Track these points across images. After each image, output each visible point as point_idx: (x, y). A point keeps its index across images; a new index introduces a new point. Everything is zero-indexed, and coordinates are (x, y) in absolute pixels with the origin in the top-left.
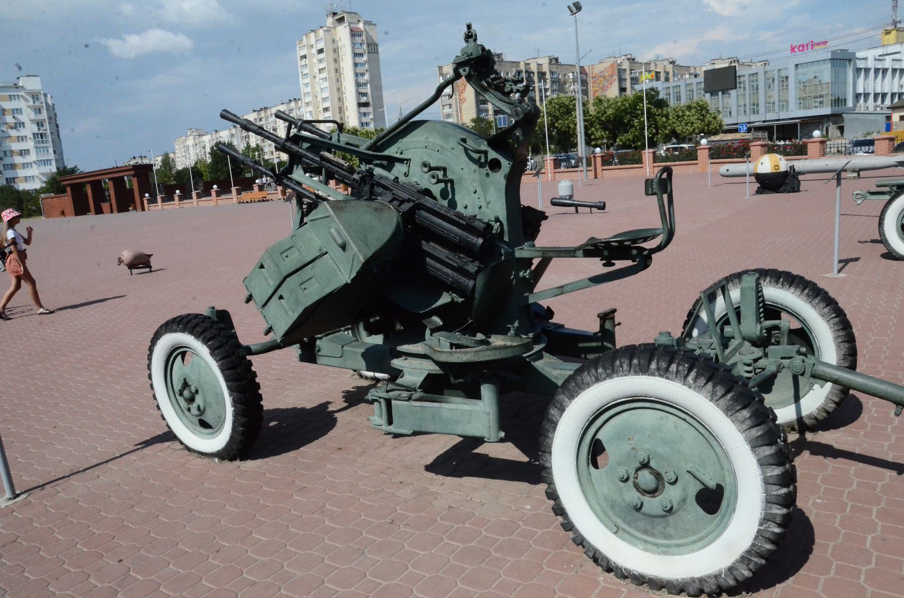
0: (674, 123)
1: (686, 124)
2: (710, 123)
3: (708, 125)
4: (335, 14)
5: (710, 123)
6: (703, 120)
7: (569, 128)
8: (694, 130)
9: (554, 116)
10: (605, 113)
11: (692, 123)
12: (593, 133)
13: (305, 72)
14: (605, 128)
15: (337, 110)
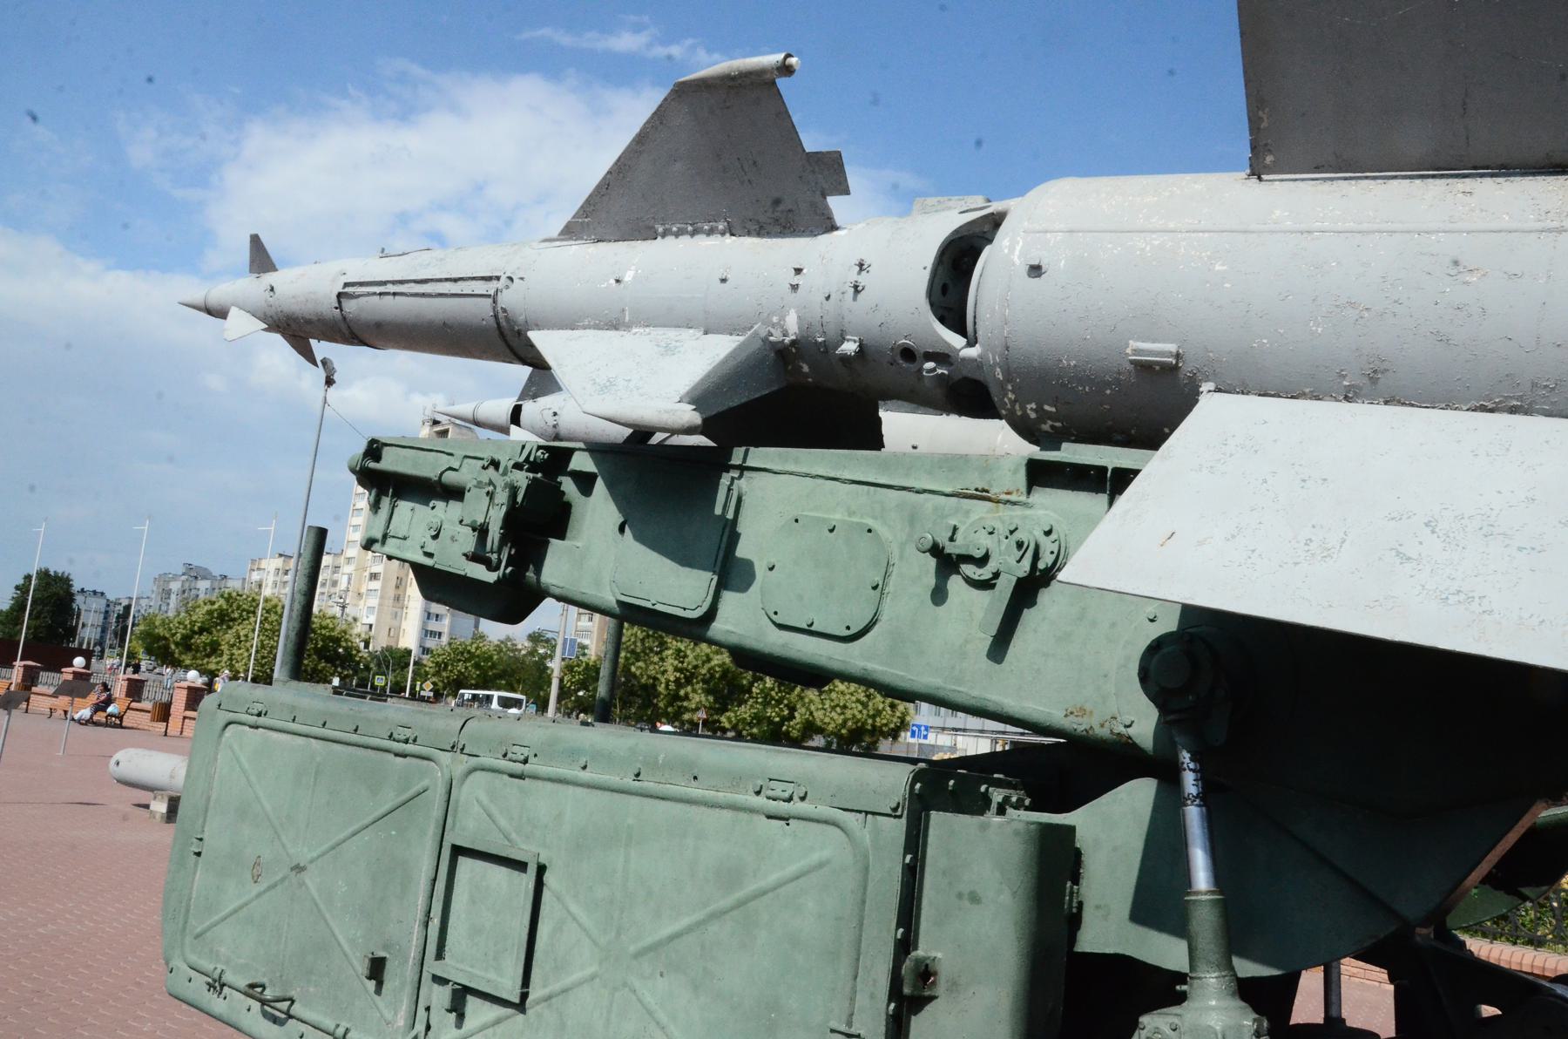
0: (811, 701)
1: (833, 708)
2: (878, 713)
3: (874, 717)
4: (436, 423)
5: (878, 713)
6: (865, 705)
7: (655, 679)
8: (845, 721)
9: (633, 652)
10: (709, 660)
11: (845, 707)
12: (686, 697)
13: (359, 506)
14: (707, 692)
15: (394, 582)
